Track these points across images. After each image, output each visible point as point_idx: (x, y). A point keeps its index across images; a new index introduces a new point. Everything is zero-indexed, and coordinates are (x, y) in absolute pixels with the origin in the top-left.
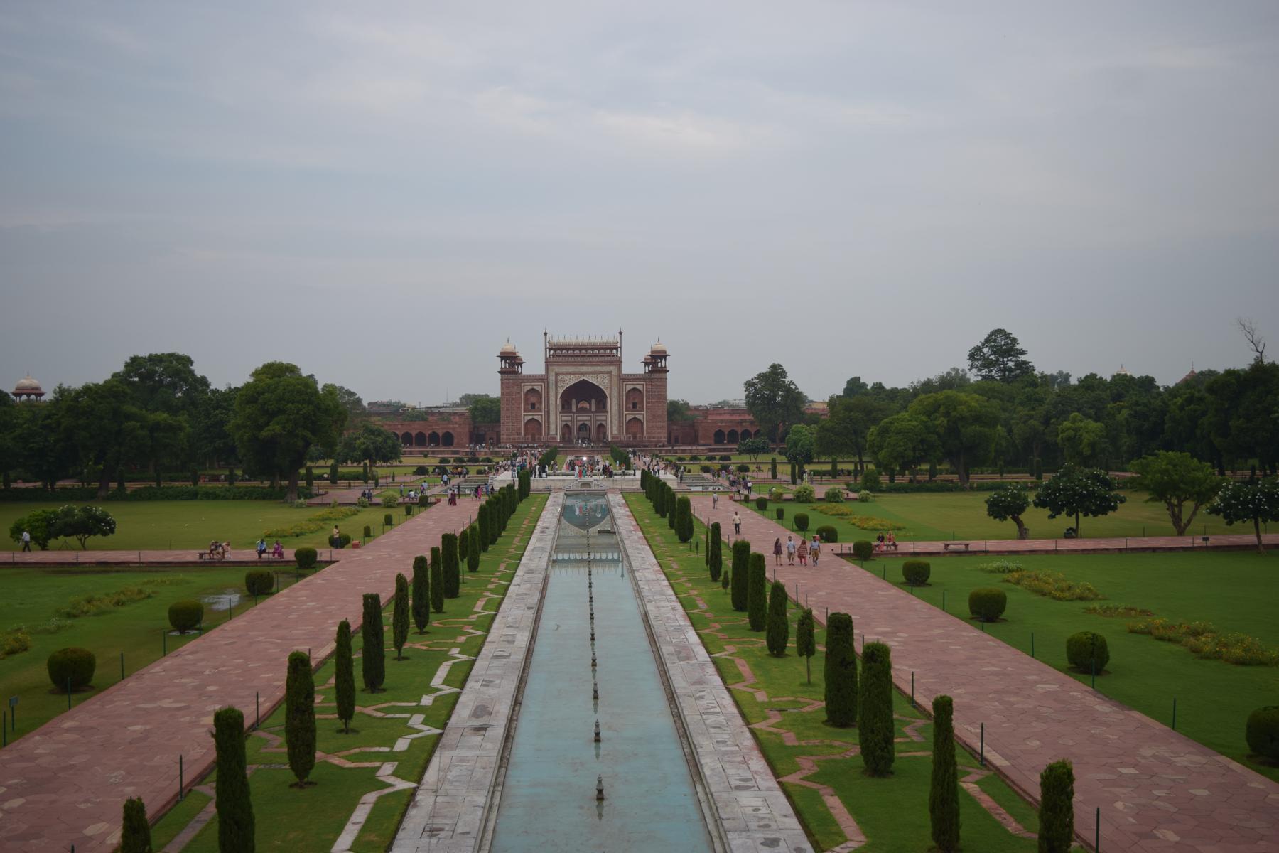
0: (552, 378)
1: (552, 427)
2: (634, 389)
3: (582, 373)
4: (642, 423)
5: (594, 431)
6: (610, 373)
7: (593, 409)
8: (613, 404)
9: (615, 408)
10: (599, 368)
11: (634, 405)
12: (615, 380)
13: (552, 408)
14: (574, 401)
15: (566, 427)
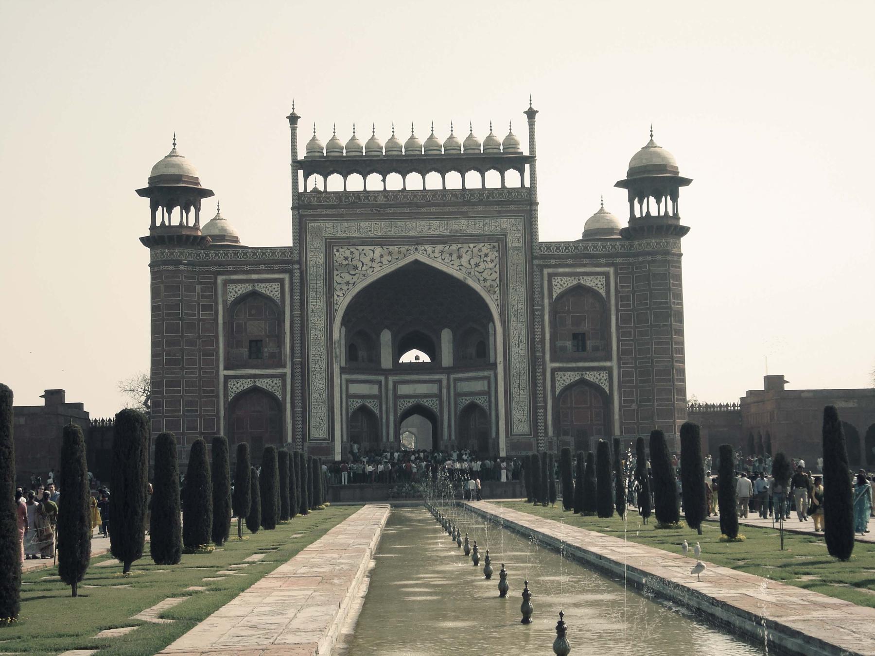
0: (315, 258)
1: (318, 413)
2: (579, 290)
3: (417, 241)
4: (607, 399)
5: (449, 431)
6: (499, 240)
7: (447, 359)
8: (510, 339)
9: (519, 351)
10: (462, 225)
11: (579, 339)
12: (517, 259)
13: (317, 352)
14: (386, 337)
15: (363, 422)
